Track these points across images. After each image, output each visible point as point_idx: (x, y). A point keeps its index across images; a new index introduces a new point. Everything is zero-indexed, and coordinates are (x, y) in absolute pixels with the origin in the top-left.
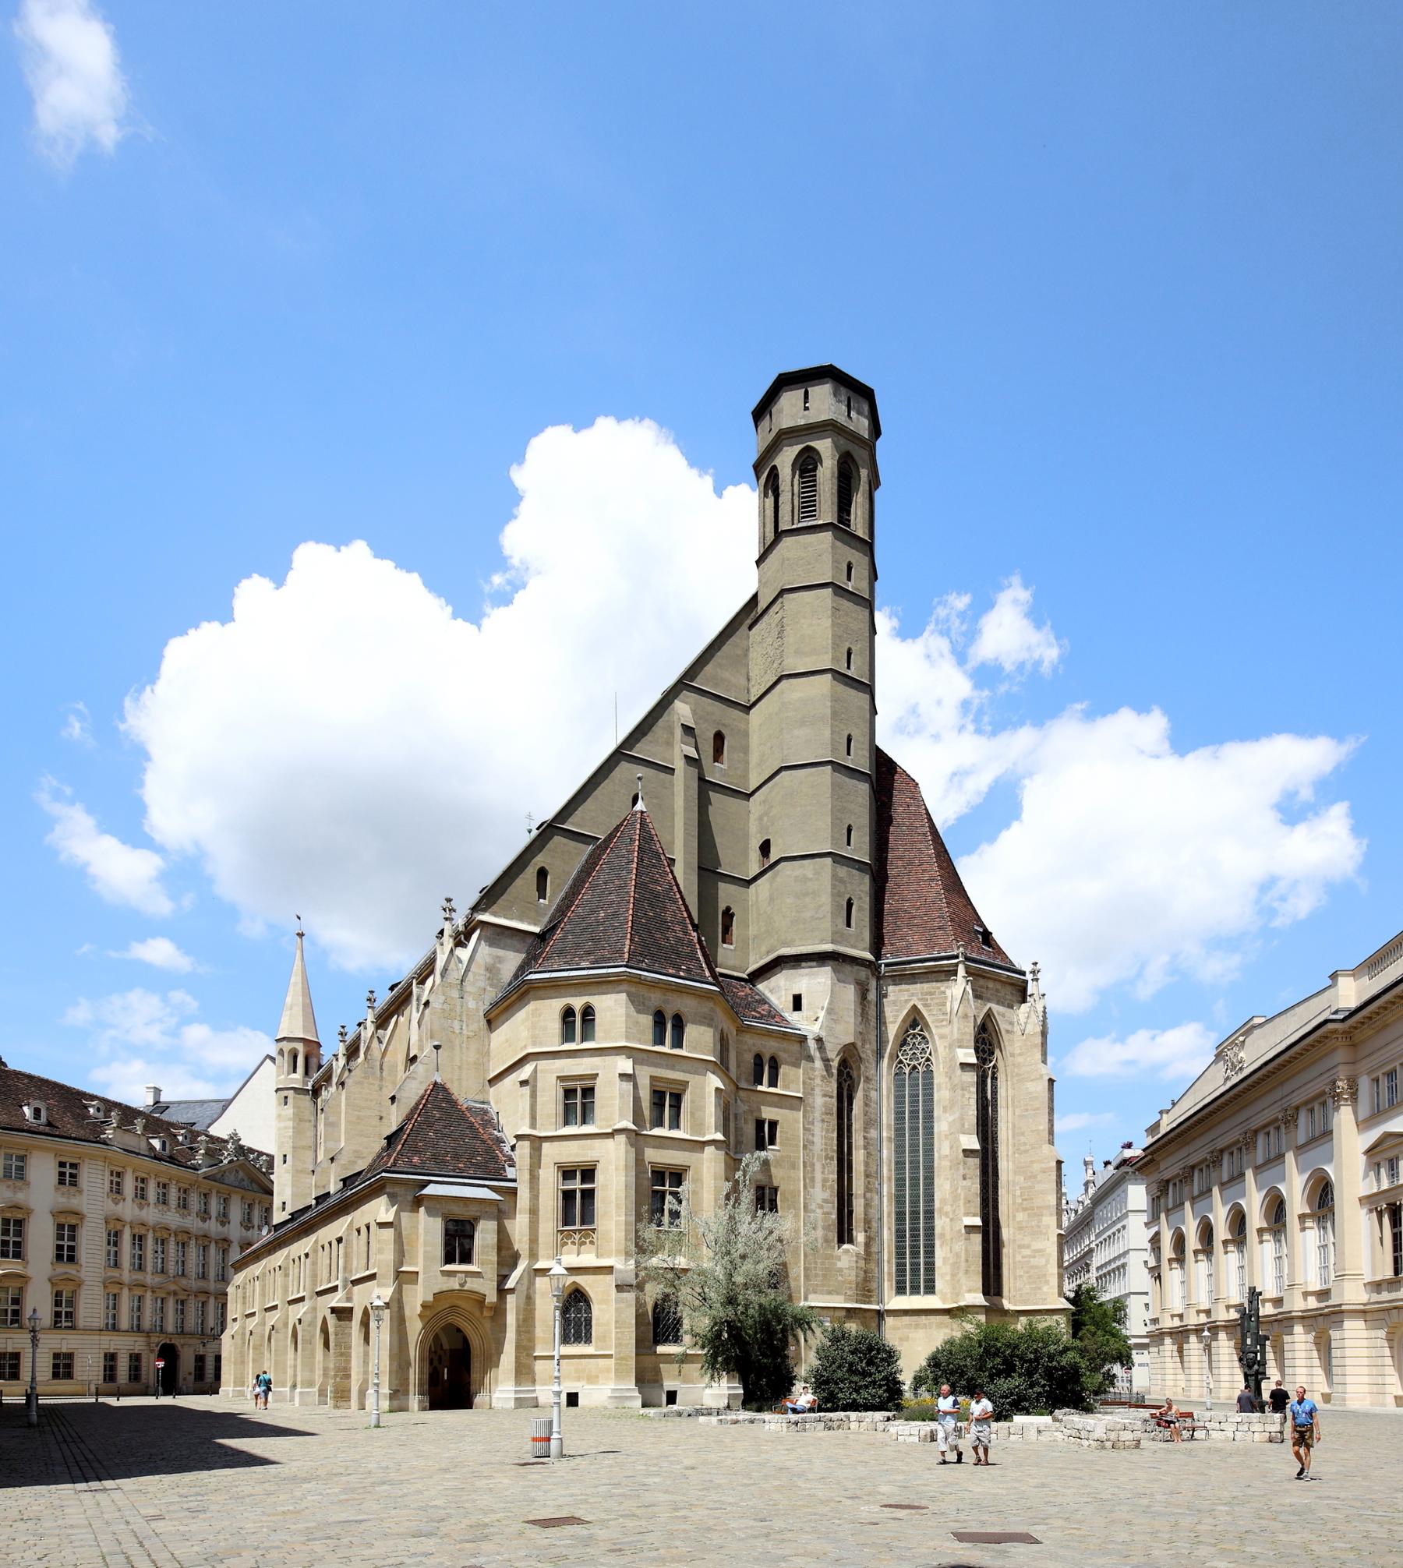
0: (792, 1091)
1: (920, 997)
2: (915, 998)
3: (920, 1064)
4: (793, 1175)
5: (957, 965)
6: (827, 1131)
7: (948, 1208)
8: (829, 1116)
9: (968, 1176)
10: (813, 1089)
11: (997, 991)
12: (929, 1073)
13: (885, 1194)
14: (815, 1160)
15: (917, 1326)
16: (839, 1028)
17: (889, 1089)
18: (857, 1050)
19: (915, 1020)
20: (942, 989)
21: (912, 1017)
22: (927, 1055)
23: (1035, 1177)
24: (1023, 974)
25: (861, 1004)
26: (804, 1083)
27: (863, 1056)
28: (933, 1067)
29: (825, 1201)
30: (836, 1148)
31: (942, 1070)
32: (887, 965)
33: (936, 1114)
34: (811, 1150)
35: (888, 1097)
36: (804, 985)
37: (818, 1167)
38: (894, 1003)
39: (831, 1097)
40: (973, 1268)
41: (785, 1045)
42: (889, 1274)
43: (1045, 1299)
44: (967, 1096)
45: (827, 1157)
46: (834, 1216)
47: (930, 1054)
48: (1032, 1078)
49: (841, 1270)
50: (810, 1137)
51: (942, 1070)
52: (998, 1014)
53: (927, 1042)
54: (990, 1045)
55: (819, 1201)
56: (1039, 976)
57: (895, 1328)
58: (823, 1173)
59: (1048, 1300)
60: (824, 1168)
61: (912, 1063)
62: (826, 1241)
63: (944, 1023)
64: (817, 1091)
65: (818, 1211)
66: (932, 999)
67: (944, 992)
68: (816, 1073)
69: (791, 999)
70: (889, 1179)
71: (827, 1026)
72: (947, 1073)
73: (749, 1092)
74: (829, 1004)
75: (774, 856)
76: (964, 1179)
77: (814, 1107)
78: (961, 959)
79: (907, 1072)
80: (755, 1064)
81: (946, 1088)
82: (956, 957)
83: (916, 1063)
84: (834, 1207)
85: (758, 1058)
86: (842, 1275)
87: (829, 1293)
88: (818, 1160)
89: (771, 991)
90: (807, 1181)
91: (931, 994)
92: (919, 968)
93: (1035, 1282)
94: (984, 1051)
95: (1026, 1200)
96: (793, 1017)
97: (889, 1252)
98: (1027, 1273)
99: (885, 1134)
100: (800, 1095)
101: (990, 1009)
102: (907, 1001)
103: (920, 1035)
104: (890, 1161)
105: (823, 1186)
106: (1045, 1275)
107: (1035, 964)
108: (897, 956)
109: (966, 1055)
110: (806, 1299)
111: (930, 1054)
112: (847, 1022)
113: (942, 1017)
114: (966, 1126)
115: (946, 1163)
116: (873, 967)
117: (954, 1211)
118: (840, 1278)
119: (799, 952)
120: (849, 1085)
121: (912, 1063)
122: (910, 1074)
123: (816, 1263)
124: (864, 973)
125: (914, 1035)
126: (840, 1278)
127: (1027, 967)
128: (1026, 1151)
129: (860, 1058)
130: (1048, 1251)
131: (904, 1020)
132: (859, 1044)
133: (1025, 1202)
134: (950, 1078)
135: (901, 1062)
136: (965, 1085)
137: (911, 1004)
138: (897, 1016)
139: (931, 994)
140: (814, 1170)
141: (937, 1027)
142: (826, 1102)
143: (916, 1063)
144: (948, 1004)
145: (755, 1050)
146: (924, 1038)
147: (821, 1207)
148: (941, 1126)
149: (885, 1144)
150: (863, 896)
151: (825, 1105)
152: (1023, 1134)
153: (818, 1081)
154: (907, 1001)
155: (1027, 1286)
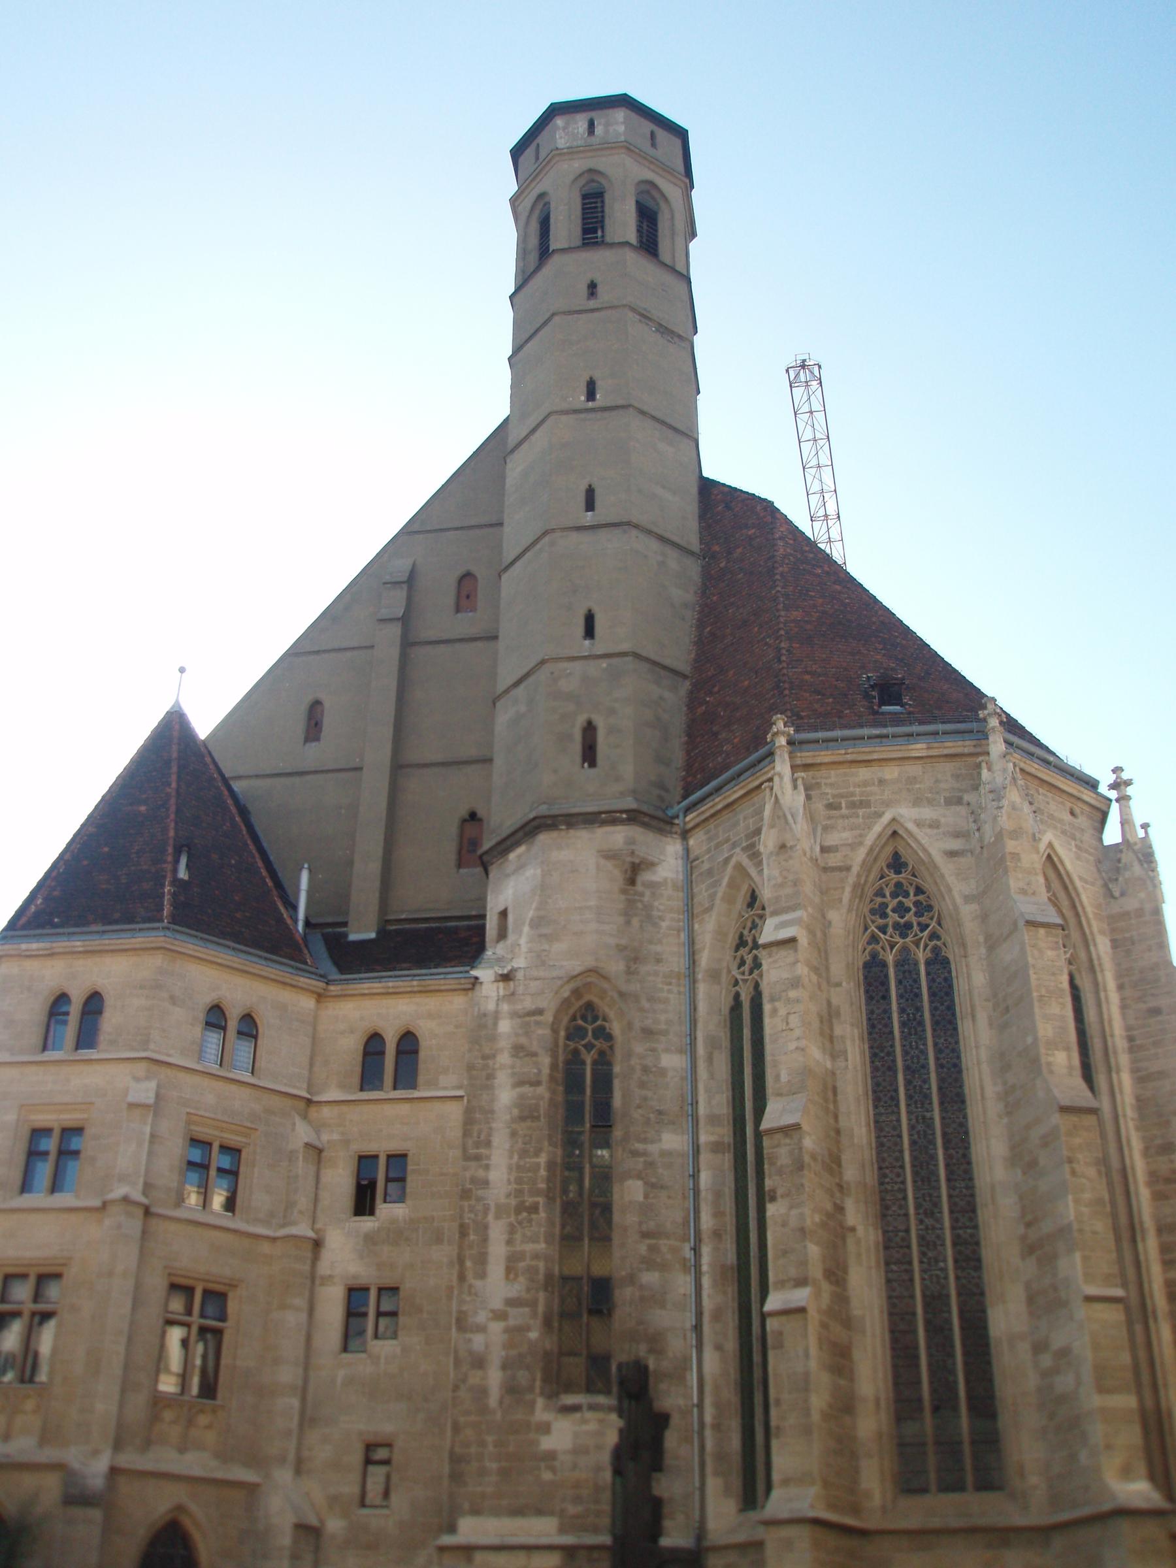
0: (445, 1088)
1: (744, 844)
2: (738, 850)
6: (524, 1153)
8: (529, 1123)
9: (779, 1192)
10: (491, 1076)
11: (912, 780)
13: (705, 1268)
14: (490, 1218)
16: (559, 947)
17: (713, 1043)
18: (605, 978)
25: (624, 892)
26: (470, 1067)
29: (511, 1302)
30: (542, 1186)
34: (479, 1199)
35: (710, 1059)
37: (497, 1232)
38: (710, 872)
39: (538, 1083)
41: (431, 1003)
42: (720, 1457)
45: (519, 1209)
46: (533, 1335)
49: (551, 1456)
52: (919, 824)
54: (919, 891)
55: (497, 1303)
58: (509, 1242)
60: (512, 1230)
62: (511, 1389)
65: (496, 1327)
68: (504, 1044)
71: (530, 951)
73: (345, 1108)
74: (538, 909)
76: (773, 1199)
77: (492, 1112)
84: (534, 1314)
86: (553, 1470)
87: (518, 1512)
88: (498, 1217)
90: (468, 1264)
94: (901, 910)
97: (717, 1405)
99: (703, 1138)
101: (894, 820)
102: (727, 861)
104: (718, 1195)
105: (509, 1270)
109: (784, 925)
110: (452, 1529)
118: (547, 1476)
120: (602, 1053)
123: (482, 1444)
124: (617, 836)
126: (547, 1476)
129: (622, 995)
131: (729, 900)
132: (616, 967)
138: (714, 894)
140: (485, 1240)
142: (522, 1097)
147: (500, 1316)
149: (705, 1157)
151: (520, 1102)
153: (504, 1058)
154: (727, 861)
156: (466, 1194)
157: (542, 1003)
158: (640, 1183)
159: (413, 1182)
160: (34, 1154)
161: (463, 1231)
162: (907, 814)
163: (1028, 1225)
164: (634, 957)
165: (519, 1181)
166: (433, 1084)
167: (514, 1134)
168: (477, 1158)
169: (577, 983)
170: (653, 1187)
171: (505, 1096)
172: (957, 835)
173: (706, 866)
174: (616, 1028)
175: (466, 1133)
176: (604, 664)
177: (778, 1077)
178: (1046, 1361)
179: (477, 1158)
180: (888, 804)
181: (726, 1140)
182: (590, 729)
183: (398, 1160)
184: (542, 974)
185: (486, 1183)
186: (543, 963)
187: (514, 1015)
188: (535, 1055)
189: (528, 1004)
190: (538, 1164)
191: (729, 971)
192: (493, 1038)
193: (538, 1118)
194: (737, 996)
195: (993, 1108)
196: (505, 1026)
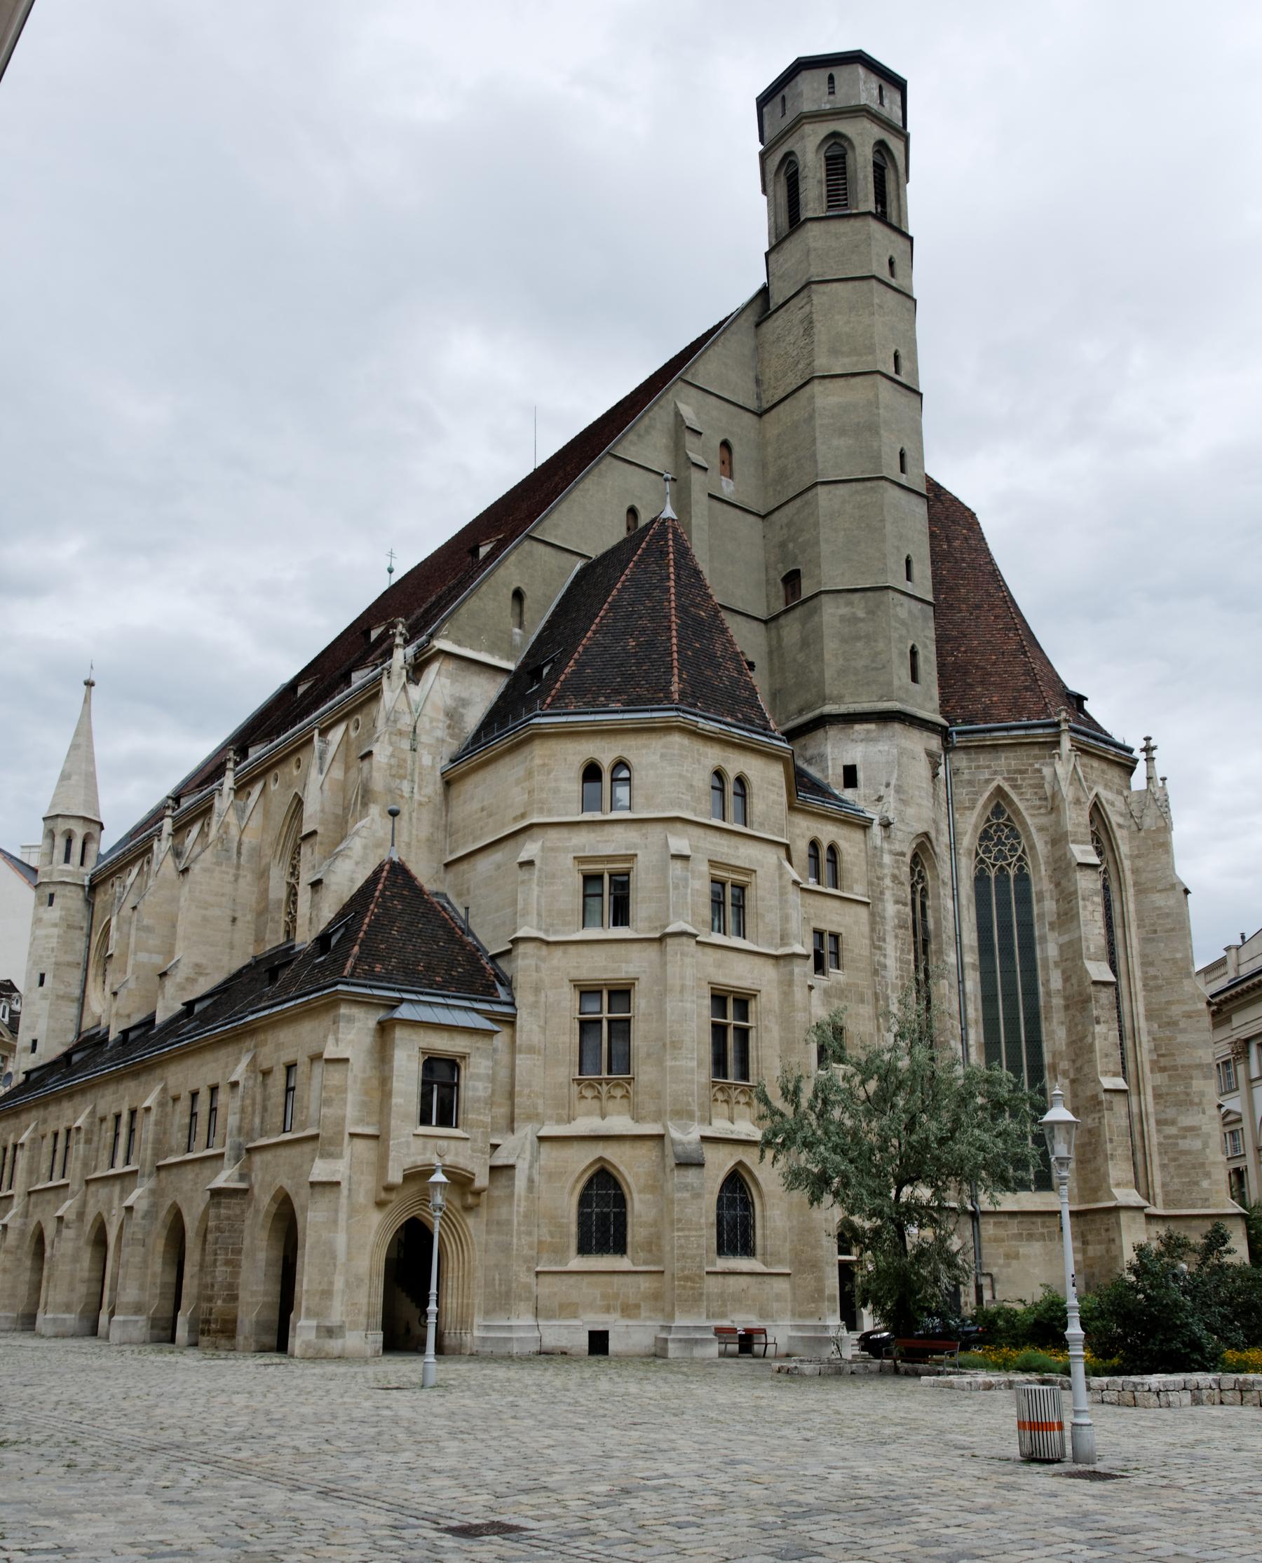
2: (999, 777)
3: (1009, 865)
4: (861, 1011)
5: (1058, 735)
6: (902, 950)
7: (1064, 1065)
8: (902, 931)
9: (1102, 1019)
10: (882, 893)
12: (1023, 878)
13: (971, 1042)
14: (889, 991)
15: (1031, 1237)
16: (910, 811)
19: (998, 805)
20: (1037, 766)
21: (995, 802)
22: (1019, 852)
23: (1175, 1024)
24: (1130, 751)
26: (870, 883)
27: (937, 850)
28: (1030, 870)
31: (1043, 873)
32: (958, 733)
33: (1037, 933)
34: (883, 977)
36: (859, 755)
38: (970, 783)
39: (905, 904)
40: (1119, 1151)
43: (1207, 1200)
44: (1090, 908)
47: (1024, 851)
48: (1159, 887)
50: (882, 959)
51: (1043, 873)
52: (1107, 801)
53: (1017, 837)
56: (1155, 754)
57: (997, 1240)
59: (1212, 1201)
61: (999, 863)
63: (1043, 811)
64: (888, 895)
66: (1023, 779)
67: (1039, 771)
68: (886, 871)
69: (841, 771)
70: (976, 1022)
71: (896, 808)
72: (1051, 877)
75: (807, 589)
76: (1098, 1023)
78: (1064, 726)
79: (993, 875)
80: (810, 856)
81: (1052, 898)
82: (1057, 725)
83: (1004, 863)
85: (814, 844)
89: (809, 761)
91: (1021, 772)
92: (1004, 738)
93: (1187, 1175)
95: (1163, 1056)
96: (848, 794)
98: (1175, 1160)
100: (866, 900)
101: (1097, 795)
102: (988, 781)
103: (1007, 826)
106: (1202, 1165)
107: (1148, 739)
108: (971, 723)
111: (1024, 851)
112: (919, 805)
113: (1038, 803)
114: (1092, 950)
115: (1057, 1001)
116: (944, 733)
117: (1079, 1070)
119: (851, 710)
120: (923, 889)
121: (999, 863)
122: (996, 877)
124: (935, 743)
125: (998, 825)
127: (1136, 744)
128: (1159, 988)
130: (1205, 1129)
131: (985, 807)
132: (933, 835)
133: (1162, 1059)
134: (1058, 885)
135: (982, 861)
136: (1087, 893)
137: (994, 784)
139: (1021, 772)
141: (1033, 815)
142: (899, 912)
143: (1004, 863)
144: (1046, 786)
145: (809, 836)
146: (1013, 829)
148: (1049, 949)
150: (928, 642)
152: (1151, 964)
153: (888, 882)
154: (988, 781)
155: (1176, 1180)
156: (876, 972)
157: (905, 850)
158: (945, 982)
159: (845, 956)
160: (717, 903)
161: (877, 1000)
162: (1106, 795)
163: (1159, 1056)
164: (938, 831)
165: (901, 969)
166: (851, 889)
167: (896, 937)
168: (880, 948)
169: (919, 841)
170: (950, 985)
171: (890, 909)
172: (1122, 815)
173: (966, 777)
174: (928, 875)
175: (873, 930)
176: (920, 605)
177: (1088, 948)
178: (1172, 1130)
179: (880, 948)
180: (1095, 782)
181: (977, 963)
182: (914, 653)
183: (835, 937)
184: (903, 828)
185: (885, 966)
186: (903, 820)
187: (891, 852)
188: (903, 884)
189: (897, 847)
190: (908, 962)
191: (977, 854)
192: (881, 865)
193: (907, 928)
194: (982, 870)
195: (1139, 985)
196: (887, 859)
